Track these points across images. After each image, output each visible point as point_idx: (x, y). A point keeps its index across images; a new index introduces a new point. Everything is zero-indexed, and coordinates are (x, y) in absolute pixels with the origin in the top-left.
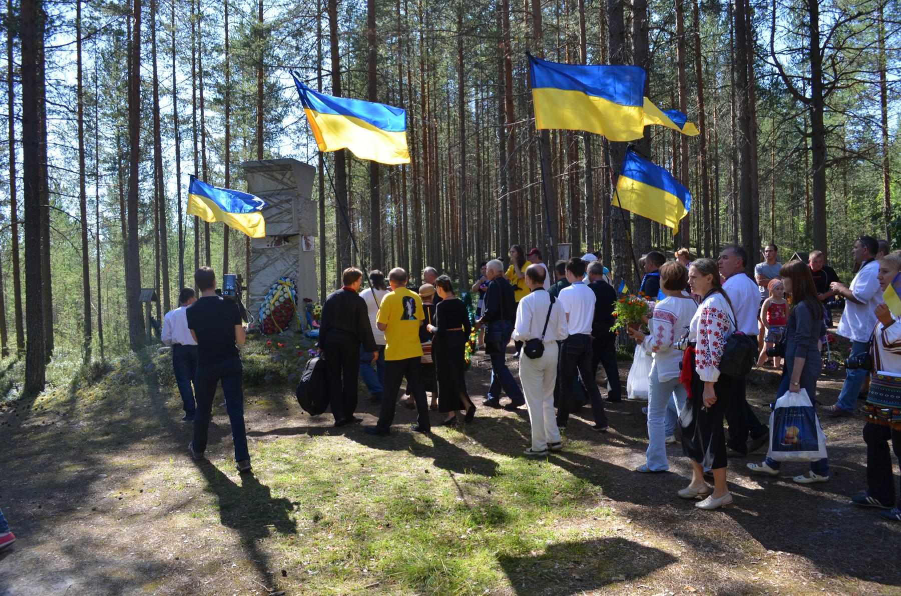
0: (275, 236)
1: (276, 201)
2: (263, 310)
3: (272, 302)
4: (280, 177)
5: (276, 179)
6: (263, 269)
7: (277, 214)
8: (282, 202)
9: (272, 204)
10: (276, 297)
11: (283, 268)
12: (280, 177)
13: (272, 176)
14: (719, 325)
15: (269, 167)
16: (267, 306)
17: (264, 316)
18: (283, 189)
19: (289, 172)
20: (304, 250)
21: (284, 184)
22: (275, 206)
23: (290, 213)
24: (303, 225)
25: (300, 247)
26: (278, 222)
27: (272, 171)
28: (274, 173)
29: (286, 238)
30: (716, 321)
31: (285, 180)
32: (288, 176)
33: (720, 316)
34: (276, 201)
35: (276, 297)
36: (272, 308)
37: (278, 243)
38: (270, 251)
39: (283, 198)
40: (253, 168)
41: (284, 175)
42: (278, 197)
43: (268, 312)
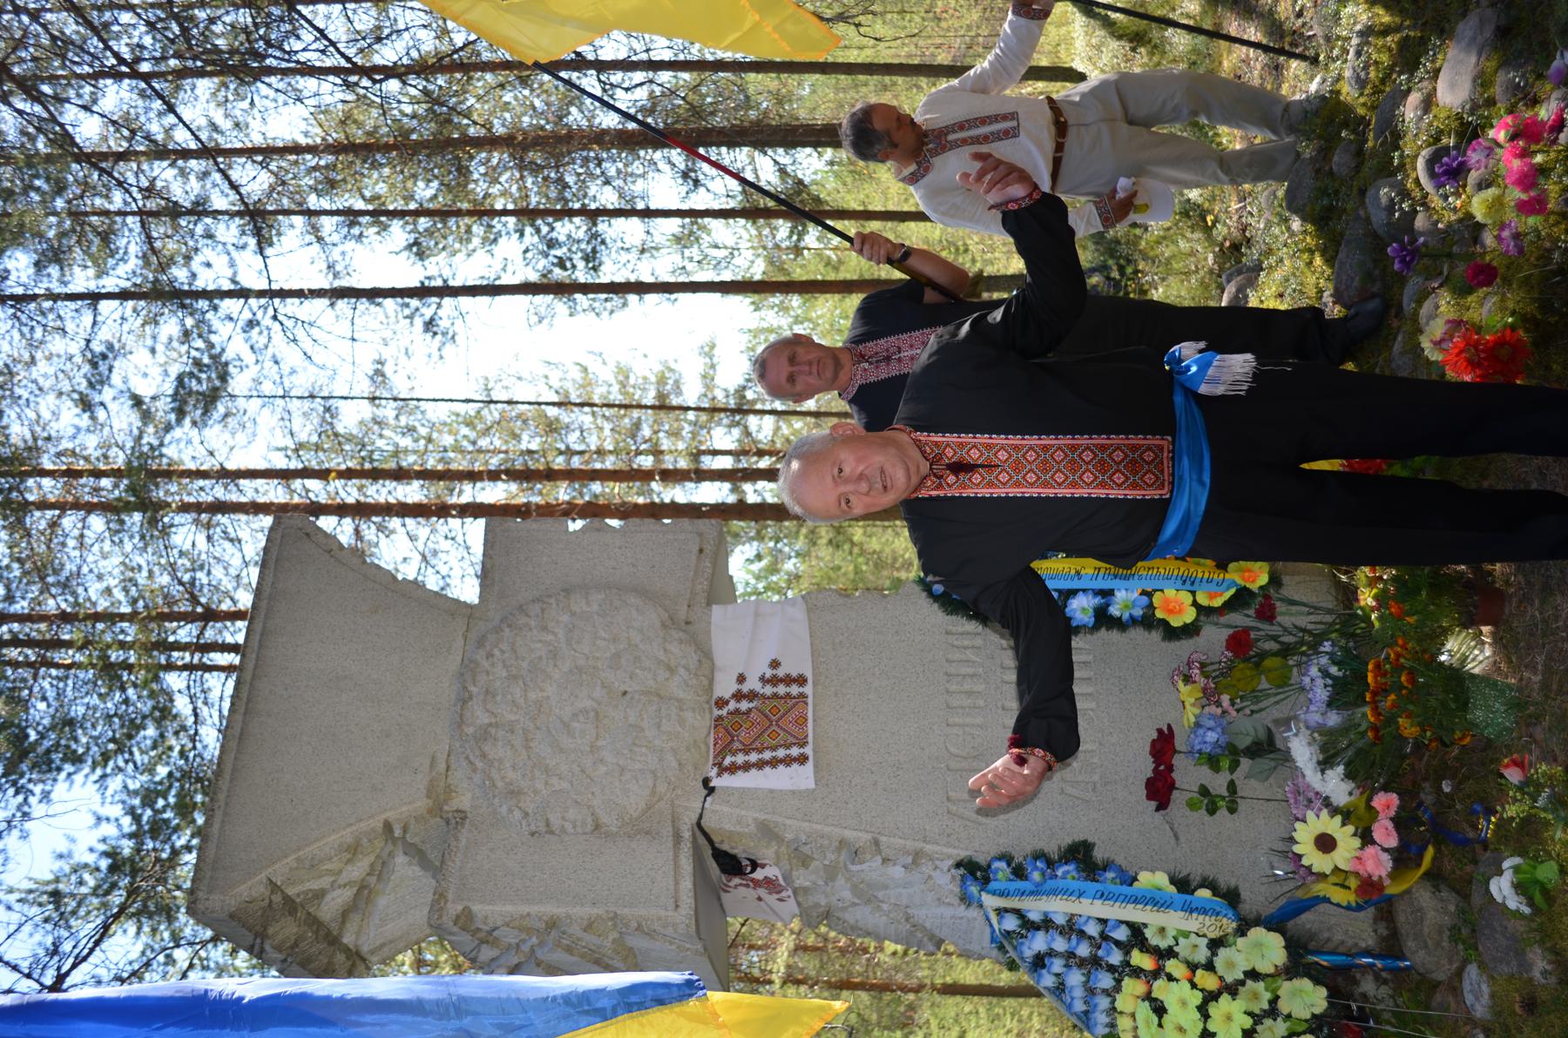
13: (345, 915)
19: (291, 891)
20: (800, 778)
24: (635, 798)
25: (793, 828)
28: (328, 910)
31: (357, 871)
32: (315, 885)
41: (319, 895)
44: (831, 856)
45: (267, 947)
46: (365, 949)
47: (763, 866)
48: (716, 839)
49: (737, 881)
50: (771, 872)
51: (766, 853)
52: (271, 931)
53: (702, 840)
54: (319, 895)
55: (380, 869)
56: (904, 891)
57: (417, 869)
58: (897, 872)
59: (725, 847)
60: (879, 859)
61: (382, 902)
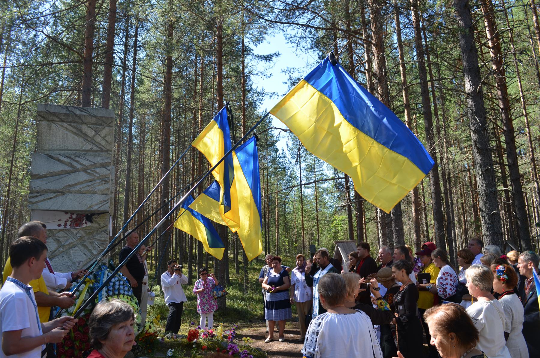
0: (72, 213)
1: (85, 163)
4: (90, 133)
5: (85, 136)
7: (87, 181)
8: (95, 165)
9: (79, 167)
11: (84, 258)
12: (90, 133)
14: (451, 280)
15: (79, 117)
18: (91, 150)
19: (107, 129)
21: (93, 142)
22: (85, 170)
23: (106, 182)
26: (86, 192)
27: (83, 123)
28: (84, 128)
29: (90, 216)
30: (449, 278)
31: (98, 139)
32: (103, 133)
33: (451, 276)
38: (62, 234)
39: (99, 160)
40: (54, 114)
44: (102, 239)
45: (83, 113)
46: (53, 125)
47: (86, 223)
48: (101, 215)
49: (74, 216)
50: (84, 225)
51: (95, 225)
52: (94, 119)
54: (97, 132)
55: (93, 142)
61: (76, 137)
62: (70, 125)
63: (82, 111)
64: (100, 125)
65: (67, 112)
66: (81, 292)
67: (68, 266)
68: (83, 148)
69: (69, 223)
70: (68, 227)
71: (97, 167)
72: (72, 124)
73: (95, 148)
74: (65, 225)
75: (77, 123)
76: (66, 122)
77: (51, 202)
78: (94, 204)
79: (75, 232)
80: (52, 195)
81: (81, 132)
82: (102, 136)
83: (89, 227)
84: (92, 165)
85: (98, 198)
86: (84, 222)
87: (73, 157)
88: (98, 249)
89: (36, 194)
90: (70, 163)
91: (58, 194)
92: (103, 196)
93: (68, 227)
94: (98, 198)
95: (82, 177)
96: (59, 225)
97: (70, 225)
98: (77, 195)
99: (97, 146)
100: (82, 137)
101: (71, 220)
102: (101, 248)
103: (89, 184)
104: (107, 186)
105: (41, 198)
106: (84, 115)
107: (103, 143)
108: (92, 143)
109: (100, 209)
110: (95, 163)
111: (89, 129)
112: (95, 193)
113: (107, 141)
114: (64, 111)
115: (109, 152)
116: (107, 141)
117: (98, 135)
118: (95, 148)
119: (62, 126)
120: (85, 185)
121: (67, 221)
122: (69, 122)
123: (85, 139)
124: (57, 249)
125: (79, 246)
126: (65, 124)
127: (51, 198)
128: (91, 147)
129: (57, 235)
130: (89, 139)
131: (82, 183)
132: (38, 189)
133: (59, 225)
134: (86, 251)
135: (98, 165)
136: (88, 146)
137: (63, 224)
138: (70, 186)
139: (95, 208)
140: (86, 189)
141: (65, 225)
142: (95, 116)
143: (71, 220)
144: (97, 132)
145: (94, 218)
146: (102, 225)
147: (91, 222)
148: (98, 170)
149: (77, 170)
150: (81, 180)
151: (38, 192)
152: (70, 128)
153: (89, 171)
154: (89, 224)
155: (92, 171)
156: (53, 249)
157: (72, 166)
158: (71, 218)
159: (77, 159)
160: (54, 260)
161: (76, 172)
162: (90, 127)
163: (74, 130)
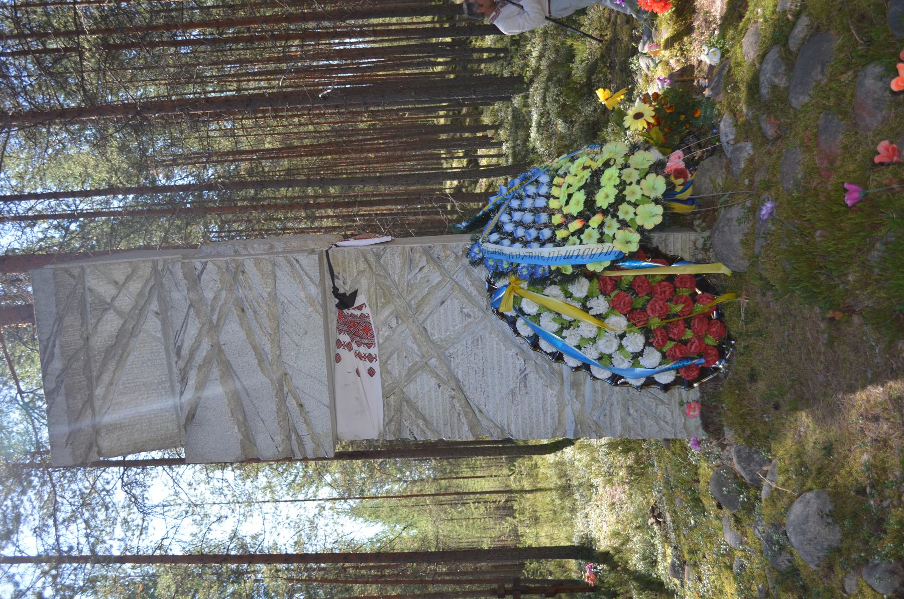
1: (193, 329)
2: (622, 364)
3: (588, 327)
4: (111, 324)
6: (460, 388)
10: (570, 312)
11: (454, 305)
12: (111, 324)
13: (109, 351)
16: (607, 345)
17: (652, 358)
21: (139, 312)
22: (214, 328)
31: (125, 302)
32: (105, 290)
34: (193, 329)
35: (570, 312)
36: (618, 322)
37: (360, 331)
42: (177, 319)
43: (635, 341)
45: (57, 351)
47: (360, 308)
48: (336, 270)
49: (345, 338)
50: (366, 311)
52: (67, 321)
53: (328, 282)
55: (139, 312)
56: (441, 309)
57: (159, 323)
58: (436, 278)
59: (339, 283)
60: (424, 258)
62: (99, 377)
63: (52, 355)
64: (83, 301)
65: (62, 391)
66: (544, 308)
67: (476, 342)
68: (159, 335)
69: (363, 350)
70: (374, 351)
71: (202, 299)
72: (95, 374)
73: (154, 306)
74: (371, 358)
75: (88, 362)
76: (91, 387)
77: (309, 404)
78: (303, 295)
79: (385, 332)
80: (292, 403)
81: (113, 347)
82: (114, 292)
83: (369, 300)
84: (198, 313)
85: (288, 288)
86: (357, 313)
87: (181, 364)
88: (425, 270)
89: (294, 442)
90: (200, 368)
91: (286, 389)
92: (279, 273)
93: (374, 351)
94: (288, 288)
95: (232, 333)
96: (371, 372)
97: (369, 346)
98: (285, 341)
99: (148, 301)
100: (127, 344)
101: (354, 345)
102: (423, 262)
103: (250, 312)
104: (249, 265)
105: (303, 429)
106: (62, 347)
107: (135, 287)
108: (140, 314)
109: (317, 279)
110: (191, 306)
111: (99, 329)
112: (274, 296)
113: (128, 278)
114: (60, 399)
115: (160, 268)
116: (128, 278)
117: (117, 303)
118: (154, 306)
119: (104, 397)
120: (254, 324)
121: (359, 355)
122: (89, 379)
123: (133, 334)
124: (433, 372)
125: (421, 318)
126: (99, 391)
127: (301, 406)
128: (151, 316)
129: (396, 373)
130: (130, 326)
131: (249, 333)
132: (278, 438)
133: (371, 372)
134: (434, 301)
135: (193, 295)
136: (152, 325)
137: (368, 365)
138: (261, 362)
139: (314, 290)
140: (265, 321)
141: (371, 358)
142: (60, 319)
143: (354, 345)
144: (105, 306)
145: (345, 289)
146: (362, 266)
147: (355, 294)
148: (209, 295)
149: (218, 349)
150: (242, 335)
151: (289, 438)
152: (106, 378)
153: (215, 317)
154: (360, 300)
155: (213, 310)
156: (433, 381)
157: (207, 362)
158: (349, 347)
159: (185, 352)
160: (460, 376)
161: (221, 351)
162: (96, 327)
163: (112, 366)
